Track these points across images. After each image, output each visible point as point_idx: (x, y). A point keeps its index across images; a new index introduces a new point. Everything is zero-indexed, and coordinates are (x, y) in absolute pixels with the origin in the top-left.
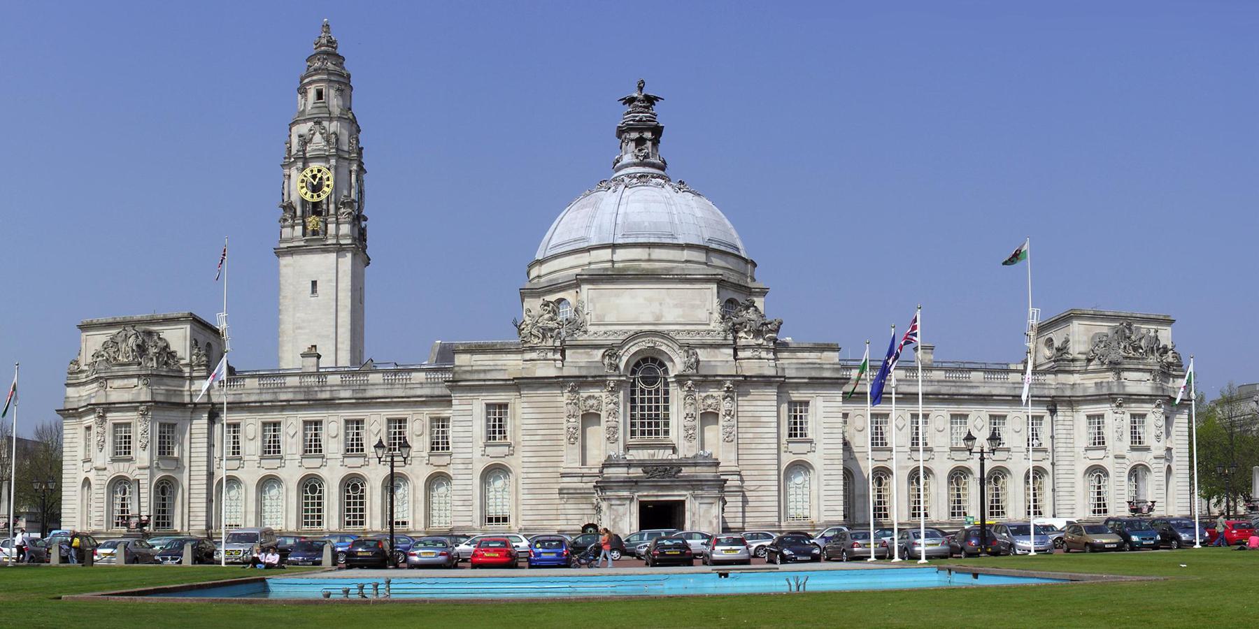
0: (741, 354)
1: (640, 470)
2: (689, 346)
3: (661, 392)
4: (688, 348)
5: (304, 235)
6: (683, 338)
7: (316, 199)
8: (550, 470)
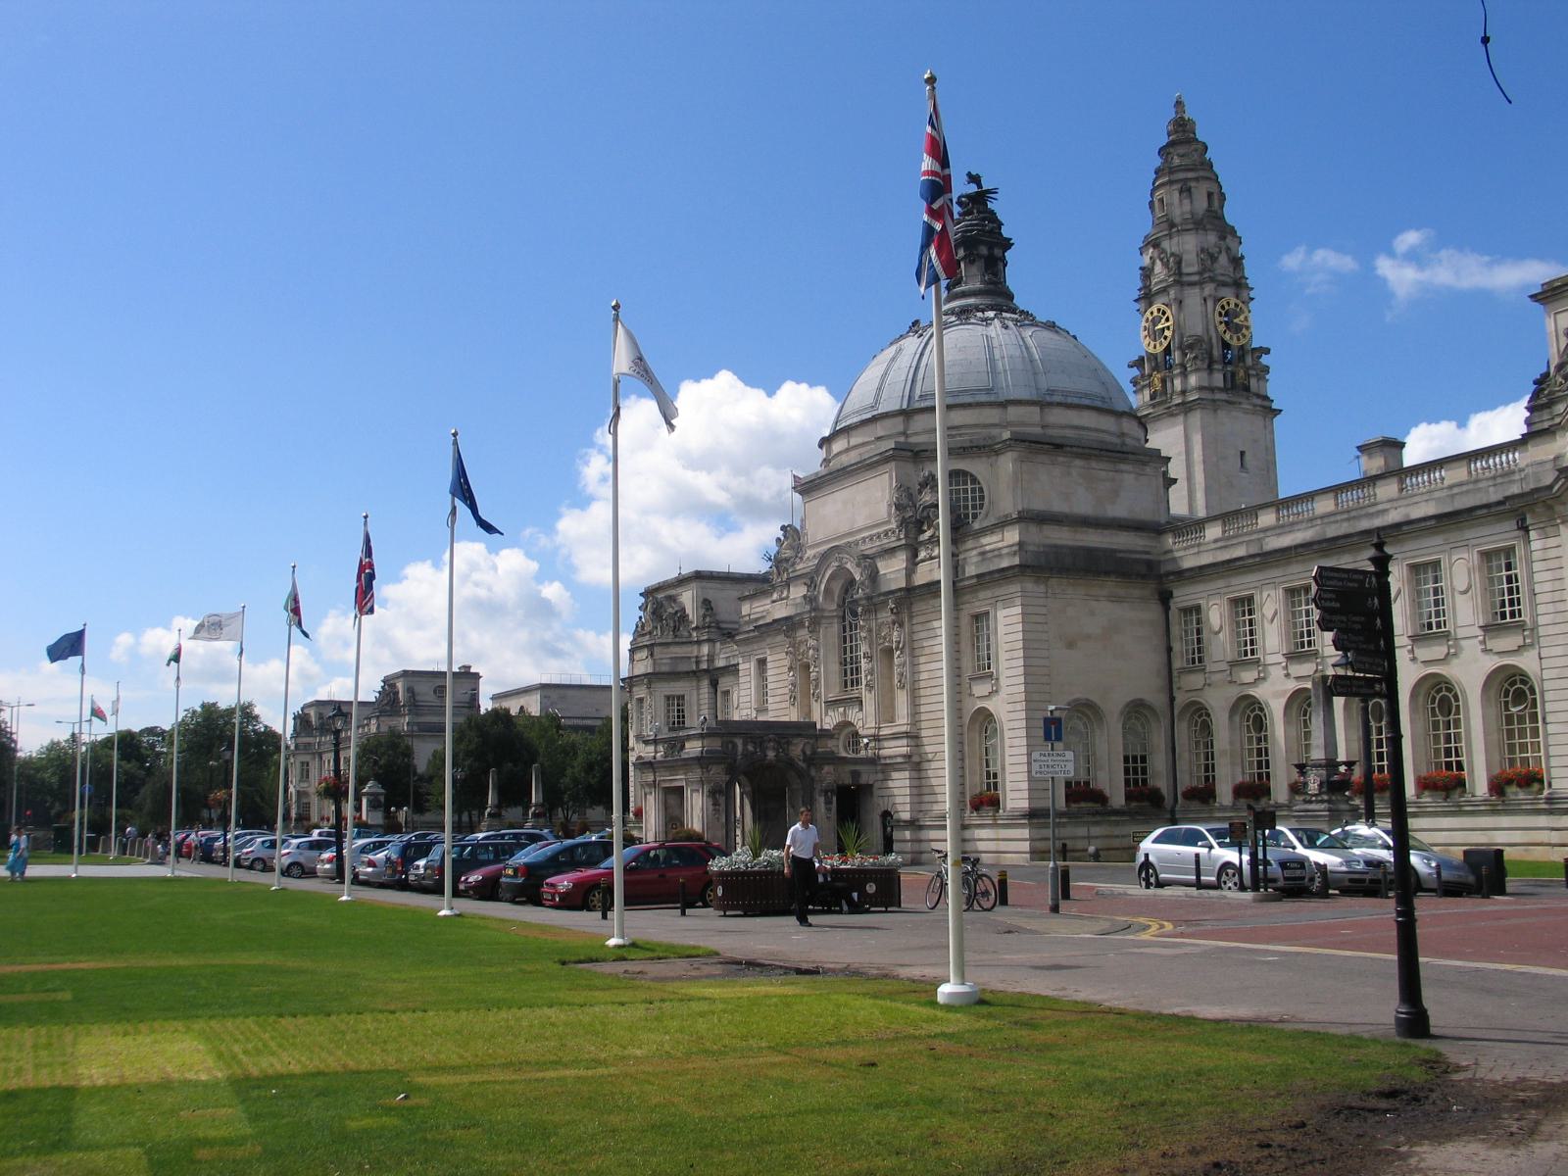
0: (922, 554)
2: (866, 557)
6: (869, 548)
7: (1160, 349)
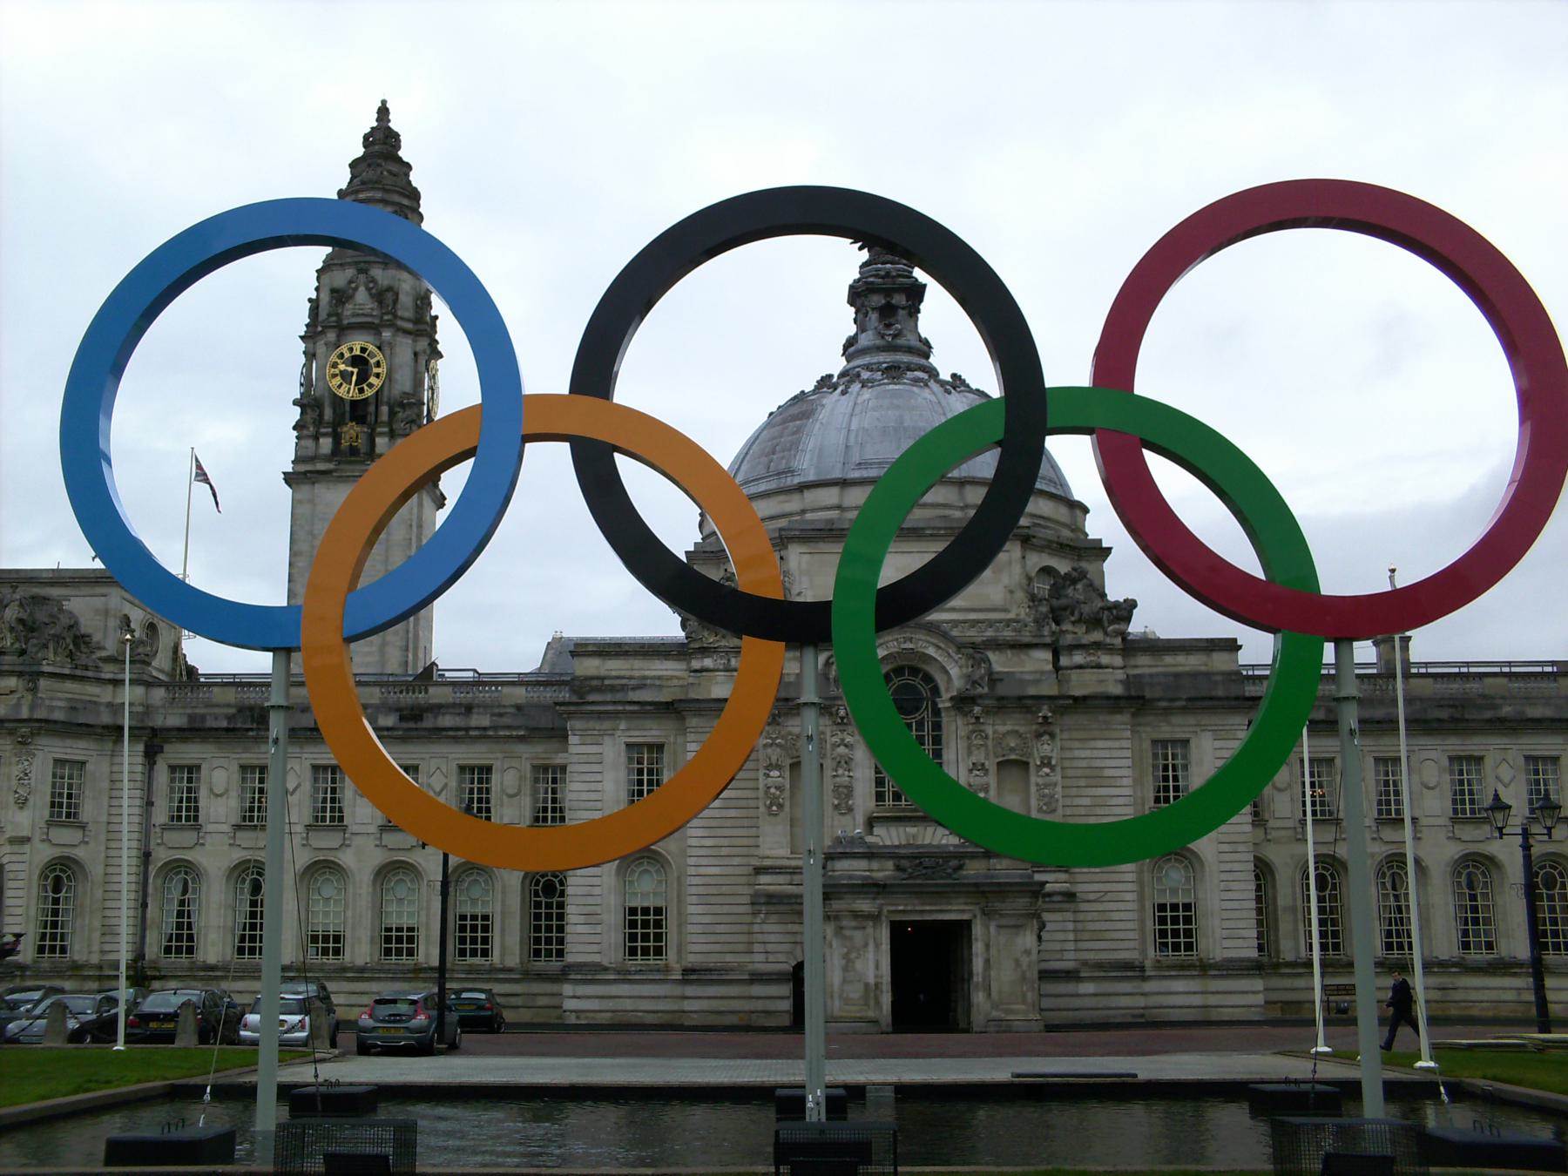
1: (890, 864)
2: (974, 646)
3: (928, 726)
4: (975, 651)
5: (336, 450)
8: (736, 861)
